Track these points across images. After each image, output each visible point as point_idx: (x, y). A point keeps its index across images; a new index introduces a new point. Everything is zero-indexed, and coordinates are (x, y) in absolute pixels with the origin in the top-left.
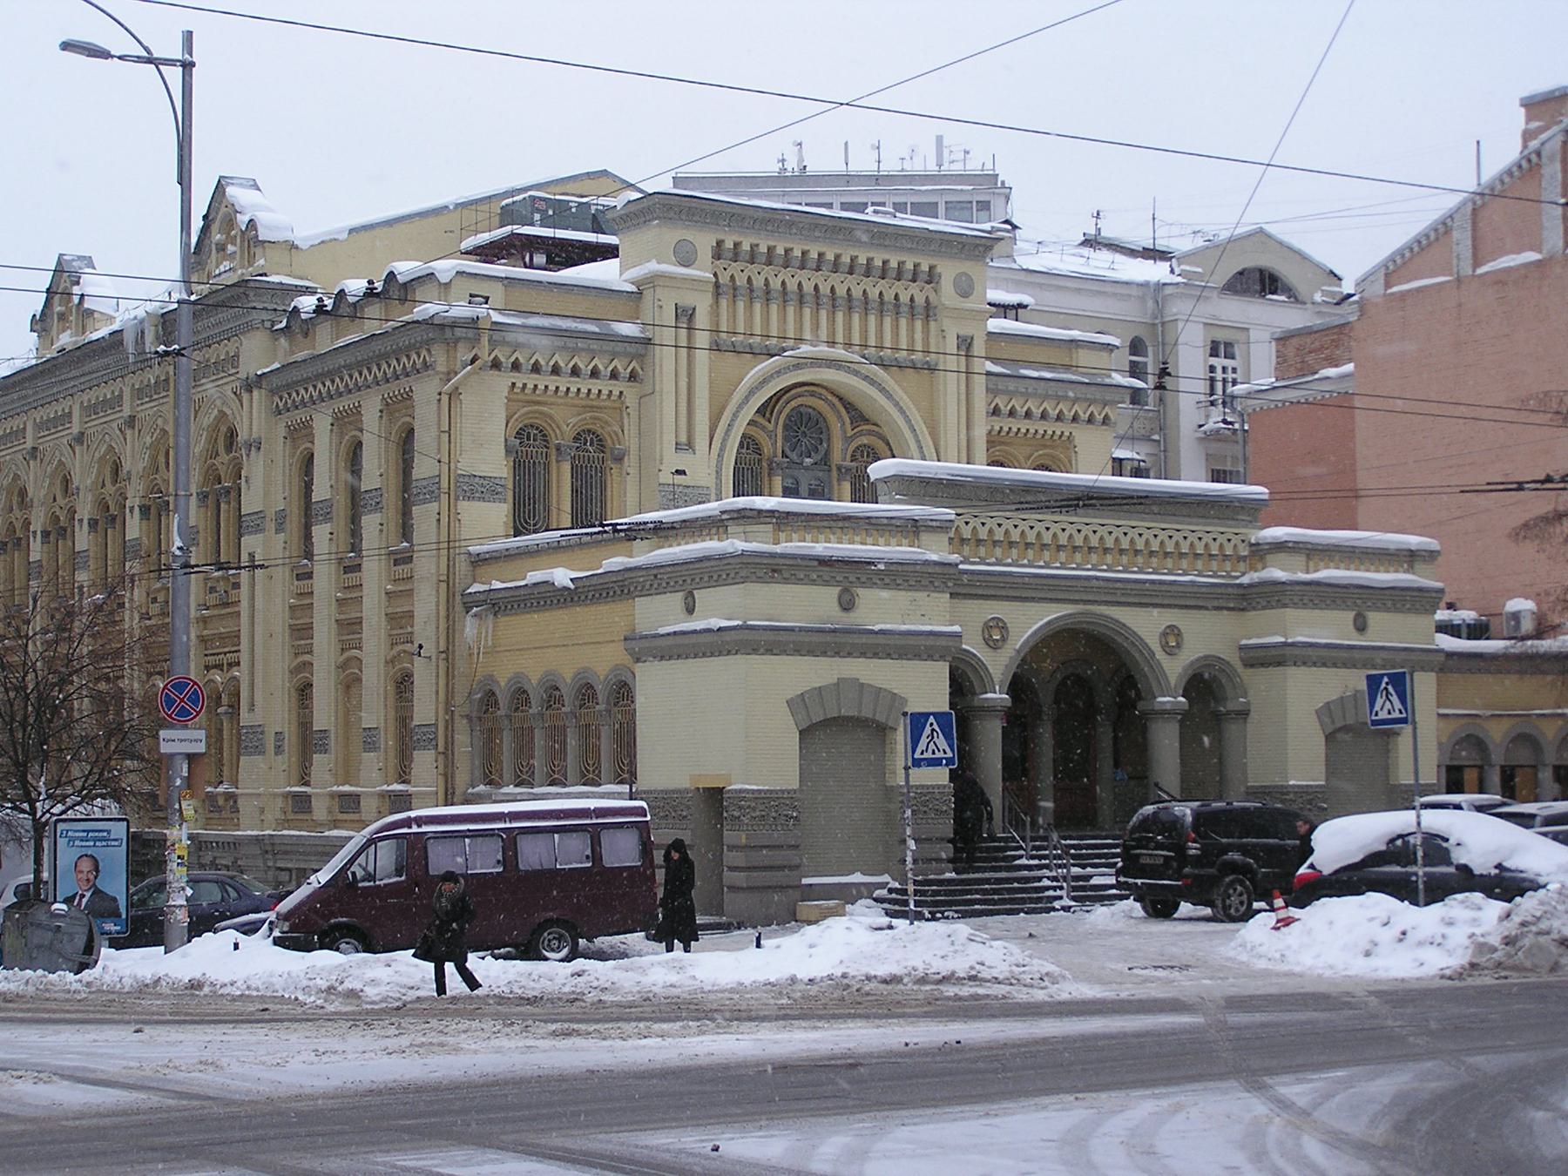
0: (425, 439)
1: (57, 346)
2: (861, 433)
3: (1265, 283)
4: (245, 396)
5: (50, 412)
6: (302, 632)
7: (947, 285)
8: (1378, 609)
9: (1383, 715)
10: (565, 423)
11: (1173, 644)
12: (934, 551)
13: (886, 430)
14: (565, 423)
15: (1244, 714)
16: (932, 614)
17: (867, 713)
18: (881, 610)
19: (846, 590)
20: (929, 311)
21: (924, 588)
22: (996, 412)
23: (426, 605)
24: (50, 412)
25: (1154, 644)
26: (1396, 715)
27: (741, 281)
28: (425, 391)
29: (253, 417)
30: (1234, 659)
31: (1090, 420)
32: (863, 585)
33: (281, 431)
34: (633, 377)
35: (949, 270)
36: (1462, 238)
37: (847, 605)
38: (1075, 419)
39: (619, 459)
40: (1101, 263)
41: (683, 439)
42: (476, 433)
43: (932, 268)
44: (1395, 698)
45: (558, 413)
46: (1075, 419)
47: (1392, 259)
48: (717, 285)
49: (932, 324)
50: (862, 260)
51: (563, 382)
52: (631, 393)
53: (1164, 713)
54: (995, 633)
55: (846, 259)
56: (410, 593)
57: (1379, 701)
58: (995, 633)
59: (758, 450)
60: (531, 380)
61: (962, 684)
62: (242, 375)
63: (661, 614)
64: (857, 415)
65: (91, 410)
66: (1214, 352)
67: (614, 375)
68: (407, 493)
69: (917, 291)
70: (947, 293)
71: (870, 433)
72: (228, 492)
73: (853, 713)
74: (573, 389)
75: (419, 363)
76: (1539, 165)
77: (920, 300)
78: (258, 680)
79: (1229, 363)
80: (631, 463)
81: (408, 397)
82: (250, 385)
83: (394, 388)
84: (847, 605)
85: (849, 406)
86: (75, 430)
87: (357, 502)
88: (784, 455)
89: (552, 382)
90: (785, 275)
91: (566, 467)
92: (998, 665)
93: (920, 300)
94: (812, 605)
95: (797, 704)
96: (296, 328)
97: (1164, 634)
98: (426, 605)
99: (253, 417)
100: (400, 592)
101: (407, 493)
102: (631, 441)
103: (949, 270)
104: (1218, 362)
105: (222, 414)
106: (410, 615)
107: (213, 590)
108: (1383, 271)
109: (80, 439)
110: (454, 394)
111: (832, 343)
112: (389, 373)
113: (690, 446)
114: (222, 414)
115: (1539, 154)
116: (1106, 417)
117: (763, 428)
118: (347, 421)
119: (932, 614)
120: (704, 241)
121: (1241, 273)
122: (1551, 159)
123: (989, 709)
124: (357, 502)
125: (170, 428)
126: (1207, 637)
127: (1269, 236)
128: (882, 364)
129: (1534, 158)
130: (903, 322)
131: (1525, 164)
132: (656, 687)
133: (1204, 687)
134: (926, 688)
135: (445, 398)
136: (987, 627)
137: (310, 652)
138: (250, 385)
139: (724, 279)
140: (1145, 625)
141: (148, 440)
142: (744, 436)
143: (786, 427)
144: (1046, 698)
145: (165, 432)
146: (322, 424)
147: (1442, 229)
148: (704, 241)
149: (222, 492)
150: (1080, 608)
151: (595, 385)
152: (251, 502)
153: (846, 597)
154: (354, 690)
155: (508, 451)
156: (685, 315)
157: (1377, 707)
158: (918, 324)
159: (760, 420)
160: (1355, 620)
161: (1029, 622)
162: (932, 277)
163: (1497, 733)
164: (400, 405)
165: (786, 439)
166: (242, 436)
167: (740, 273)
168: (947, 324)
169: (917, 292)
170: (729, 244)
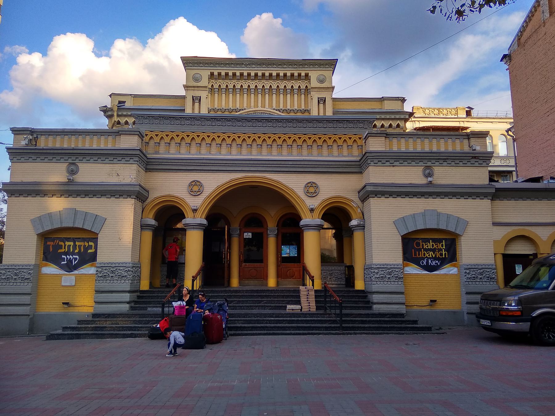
15: (362, 227)
30: (355, 198)
35: (314, 75)
43: (307, 75)
54: (195, 188)
58: (195, 188)
70: (314, 83)
84: (73, 172)
93: (303, 87)
103: (314, 75)
120: (205, 73)
140: (293, 184)
148: (205, 73)
153: (73, 167)
160: (424, 171)
163: (543, 235)
170: (216, 73)
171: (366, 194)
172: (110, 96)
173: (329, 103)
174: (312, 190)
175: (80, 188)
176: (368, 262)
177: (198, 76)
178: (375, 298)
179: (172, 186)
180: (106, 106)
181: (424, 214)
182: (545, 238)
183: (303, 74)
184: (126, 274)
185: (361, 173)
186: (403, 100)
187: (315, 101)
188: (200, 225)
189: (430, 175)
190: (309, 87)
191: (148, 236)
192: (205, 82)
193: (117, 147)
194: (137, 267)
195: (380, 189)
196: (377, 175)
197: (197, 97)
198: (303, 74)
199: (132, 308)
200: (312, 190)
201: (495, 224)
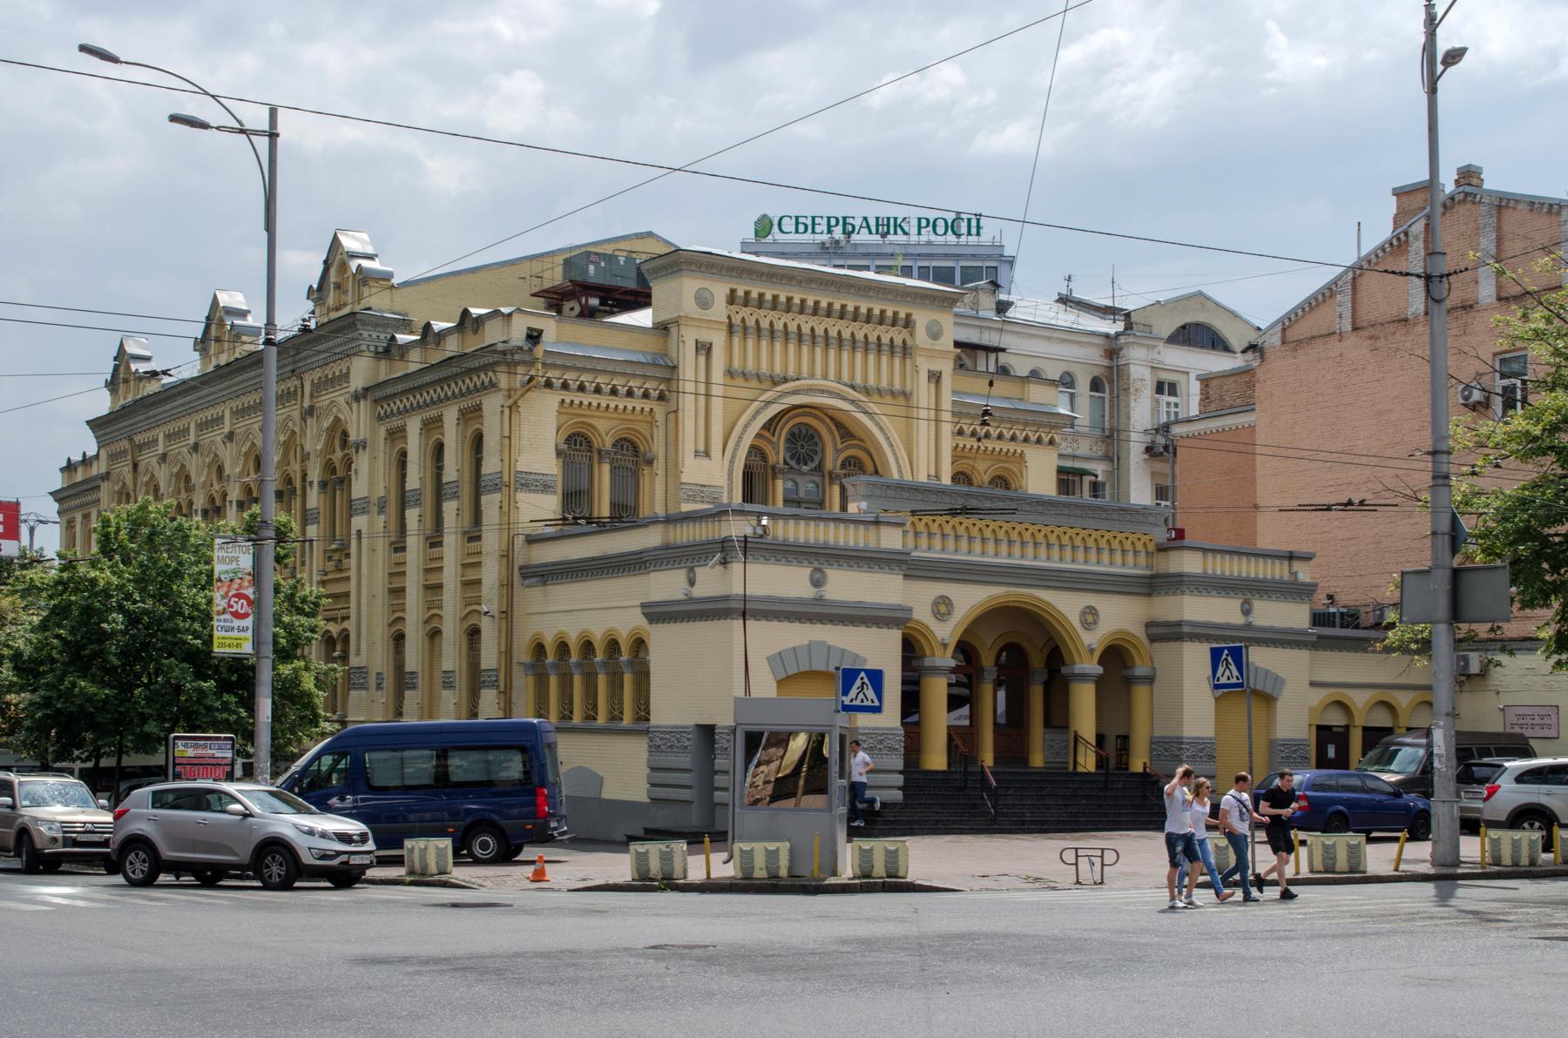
0: (491, 442)
1: (214, 363)
2: (847, 447)
3: (1198, 335)
4: (355, 406)
5: (209, 414)
6: (398, 592)
9: (1223, 680)
10: (606, 431)
11: (1093, 621)
12: (891, 539)
13: (869, 445)
14: (606, 431)
15: (1150, 680)
16: (884, 589)
18: (845, 586)
19: (816, 569)
20: (906, 351)
22: (960, 433)
23: (491, 574)
24: (209, 414)
25: (1075, 620)
26: (1234, 681)
27: (751, 322)
28: (492, 404)
29: (359, 422)
30: (1139, 632)
31: (1039, 441)
33: (382, 433)
34: (661, 397)
35: (922, 318)
36: (1345, 299)
38: (1026, 440)
39: (650, 462)
40: (1067, 318)
41: (701, 448)
42: (533, 437)
43: (908, 316)
44: (1233, 668)
45: (602, 425)
46: (1026, 440)
47: (1287, 316)
48: (731, 326)
49: (908, 361)
50: (850, 308)
51: (604, 400)
52: (659, 410)
53: (1084, 677)
54: (943, 607)
55: (837, 307)
56: (478, 564)
57: (1221, 669)
58: (943, 607)
59: (764, 457)
60: (578, 398)
61: (911, 649)
62: (352, 389)
63: (667, 585)
64: (845, 431)
65: (240, 413)
66: (1160, 388)
67: (646, 395)
68: (478, 489)
69: (898, 335)
70: (921, 336)
71: (855, 446)
72: (342, 481)
73: (823, 668)
74: (612, 406)
75: (486, 381)
76: (1407, 242)
77: (898, 341)
78: (364, 630)
79: (1172, 399)
80: (659, 465)
81: (478, 408)
82: (357, 397)
83: (467, 403)
85: (839, 425)
86: (227, 430)
87: (440, 492)
88: (786, 463)
89: (595, 400)
90: (787, 318)
91: (606, 468)
92: (946, 632)
93: (898, 341)
94: (790, 581)
96: (394, 351)
97: (1083, 613)
98: (491, 574)
99: (359, 422)
100: (471, 564)
101: (478, 489)
102: (658, 448)
103: (922, 318)
104: (1166, 398)
105: (337, 420)
106: (478, 582)
107: (330, 559)
108: (1279, 327)
109: (230, 436)
110: (513, 408)
111: (825, 377)
112: (464, 389)
113: (707, 454)
114: (337, 420)
115: (1406, 234)
116: (1051, 442)
117: (770, 441)
118: (432, 425)
119: (884, 589)
120: (719, 290)
121: (1183, 327)
122: (1416, 238)
123: (936, 670)
124: (440, 492)
125: (297, 429)
126: (1119, 616)
127: (1208, 299)
128: (867, 391)
129: (1402, 237)
130: (884, 359)
131: (1395, 242)
132: (666, 644)
133: (1116, 656)
134: (880, 650)
135: (507, 411)
136: (936, 604)
137: (403, 610)
138: (357, 397)
139: (737, 320)
140: (1066, 605)
141: (282, 438)
142: (752, 447)
143: (787, 440)
144: (987, 661)
145: (294, 432)
146: (414, 426)
147: (1328, 293)
148: (720, 290)
149: (337, 480)
150: (1013, 589)
151: (630, 403)
152: (359, 489)
153: (818, 575)
154: (437, 640)
155: (559, 453)
156: (705, 349)
157: (1219, 674)
158: (897, 361)
159: (766, 433)
161: (969, 599)
162: (908, 323)
163: (1360, 700)
164: (471, 414)
165: (787, 449)
166: (352, 438)
167: (750, 315)
168: (920, 360)
170: (740, 293)
174: (1090, 619)
175: (830, 611)
176: (1159, 732)
177: (707, 295)
182: (1360, 706)
183: (902, 315)
185: (1150, 595)
187: (924, 376)
189: (1246, 612)
190: (909, 343)
192: (720, 310)
193: (872, 545)
195: (1198, 630)
197: (703, 345)
198: (902, 315)
200: (1090, 617)
201: (1313, 684)
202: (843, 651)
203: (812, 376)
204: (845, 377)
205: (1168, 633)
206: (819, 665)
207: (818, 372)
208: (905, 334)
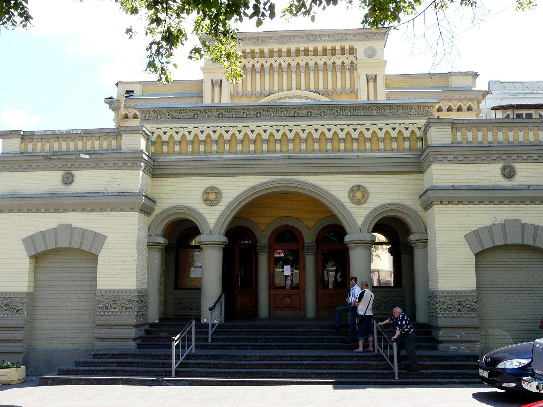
7: (360, 53)
8: (525, 161)
11: (358, 197)
15: (425, 242)
17: (75, 245)
21: (119, 168)
25: (343, 197)
30: (414, 204)
32: (78, 168)
37: (68, 180)
49: (355, 72)
58: (212, 196)
69: (347, 59)
93: (347, 62)
95: (29, 241)
111: (298, 88)
140: (336, 188)
162: (352, 51)
169: (347, 59)
171: (429, 198)
172: (117, 84)
173: (381, 82)
178: (442, 335)
179: (184, 194)
180: (111, 98)
181: (504, 226)
184: (131, 305)
186: (475, 75)
188: (218, 243)
191: (157, 256)
194: (142, 296)
196: (441, 174)
199: (139, 346)
200: (359, 195)
202: (84, 231)
203: (289, 89)
204: (312, 87)
205: (429, 198)
206: (63, 244)
207: (294, 86)
208: (352, 58)
